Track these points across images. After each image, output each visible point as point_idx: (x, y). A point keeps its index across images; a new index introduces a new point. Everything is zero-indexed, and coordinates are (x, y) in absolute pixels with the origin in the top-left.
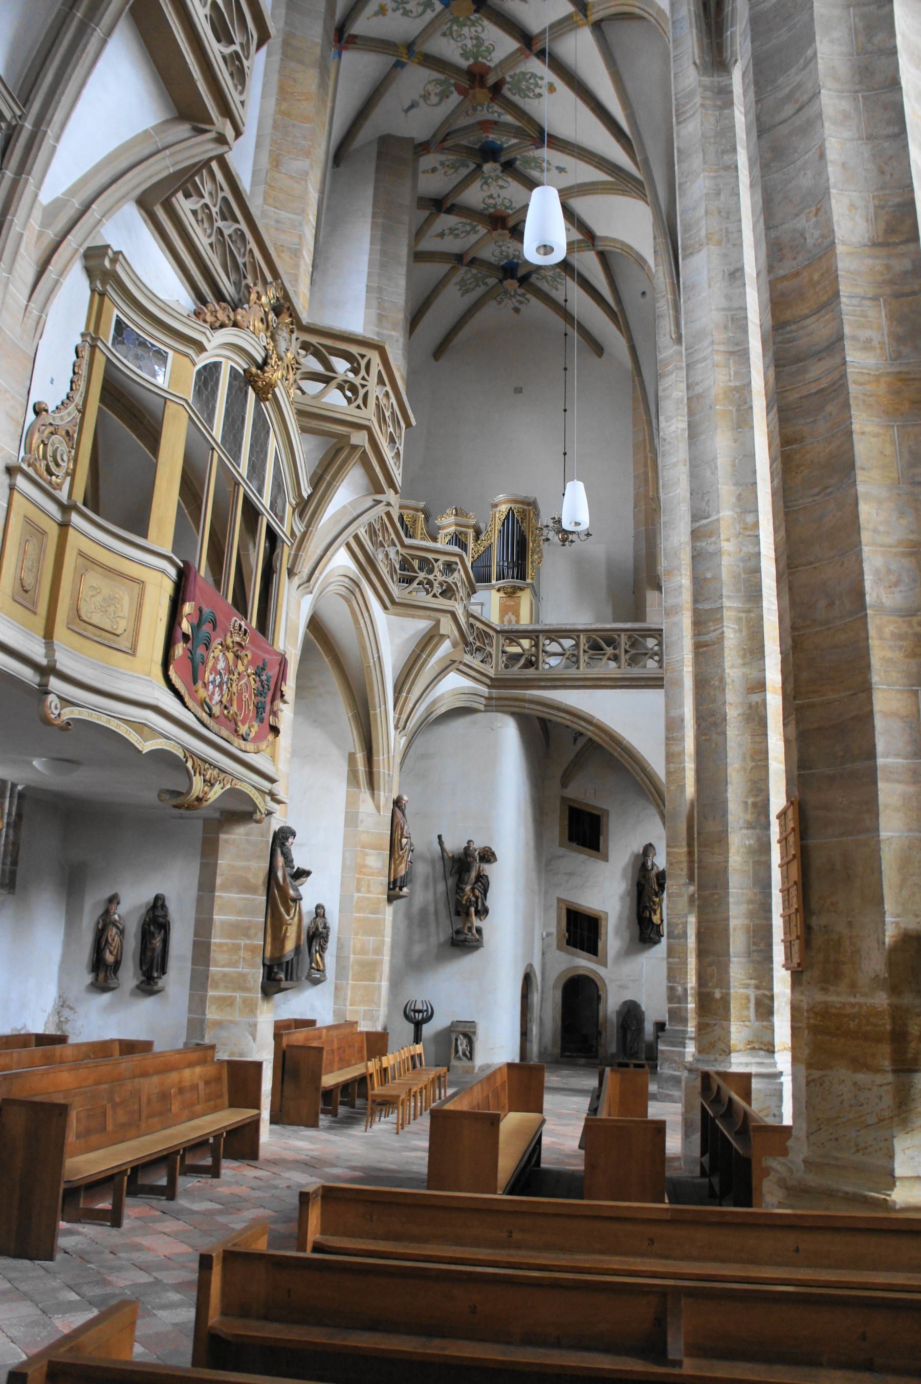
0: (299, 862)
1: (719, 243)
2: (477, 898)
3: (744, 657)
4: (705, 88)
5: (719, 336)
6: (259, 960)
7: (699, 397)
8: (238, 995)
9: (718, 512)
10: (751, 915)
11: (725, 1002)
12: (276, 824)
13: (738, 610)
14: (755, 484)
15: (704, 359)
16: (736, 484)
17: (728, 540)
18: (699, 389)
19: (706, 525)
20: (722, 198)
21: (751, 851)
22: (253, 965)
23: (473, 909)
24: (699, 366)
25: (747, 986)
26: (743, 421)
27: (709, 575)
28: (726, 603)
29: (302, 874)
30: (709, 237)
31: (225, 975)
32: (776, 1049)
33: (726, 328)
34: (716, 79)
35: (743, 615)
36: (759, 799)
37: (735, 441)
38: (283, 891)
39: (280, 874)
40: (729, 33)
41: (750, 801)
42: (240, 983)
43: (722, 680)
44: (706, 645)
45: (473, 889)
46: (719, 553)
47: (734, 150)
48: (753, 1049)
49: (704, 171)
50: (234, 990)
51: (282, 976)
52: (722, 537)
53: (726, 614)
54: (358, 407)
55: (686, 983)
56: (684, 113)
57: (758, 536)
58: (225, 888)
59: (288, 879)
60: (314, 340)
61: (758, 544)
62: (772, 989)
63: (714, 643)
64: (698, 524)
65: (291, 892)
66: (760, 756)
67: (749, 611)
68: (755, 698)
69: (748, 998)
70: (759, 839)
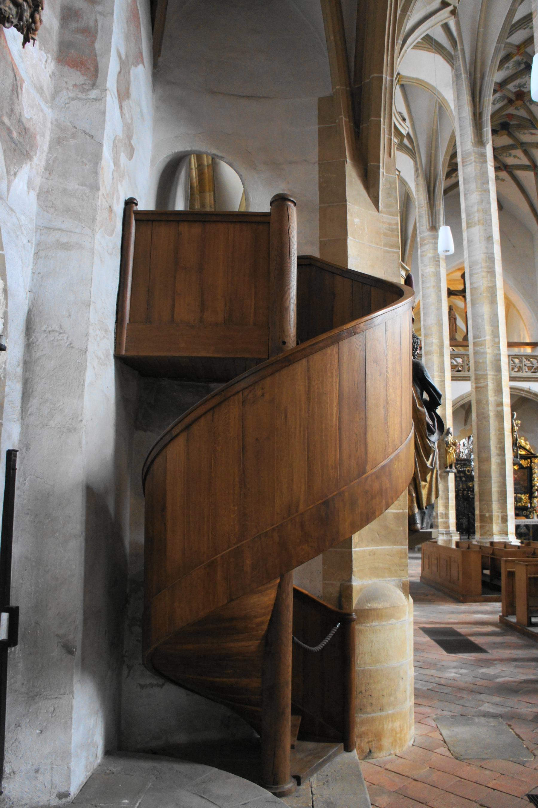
1: (483, 225)
3: (495, 393)
4: (475, 152)
5: (484, 265)
7: (475, 289)
9: (485, 337)
10: (499, 487)
11: (491, 518)
13: (493, 375)
14: (498, 326)
15: (477, 273)
16: (491, 326)
17: (489, 348)
18: (475, 285)
19: (479, 341)
20: (484, 204)
21: (499, 464)
24: (475, 275)
25: (498, 512)
26: (493, 301)
27: (481, 361)
28: (489, 372)
30: (479, 221)
32: (509, 533)
33: (486, 261)
34: (480, 149)
35: (495, 377)
36: (501, 445)
37: (491, 308)
40: (485, 129)
41: (498, 446)
43: (487, 401)
44: (480, 387)
46: (485, 353)
47: (488, 183)
48: (501, 534)
49: (476, 191)
53: (489, 377)
55: (438, 511)
56: (466, 162)
57: (499, 347)
62: (506, 513)
63: (484, 387)
64: (476, 340)
66: (501, 430)
67: (497, 376)
69: (499, 516)
70: (501, 460)
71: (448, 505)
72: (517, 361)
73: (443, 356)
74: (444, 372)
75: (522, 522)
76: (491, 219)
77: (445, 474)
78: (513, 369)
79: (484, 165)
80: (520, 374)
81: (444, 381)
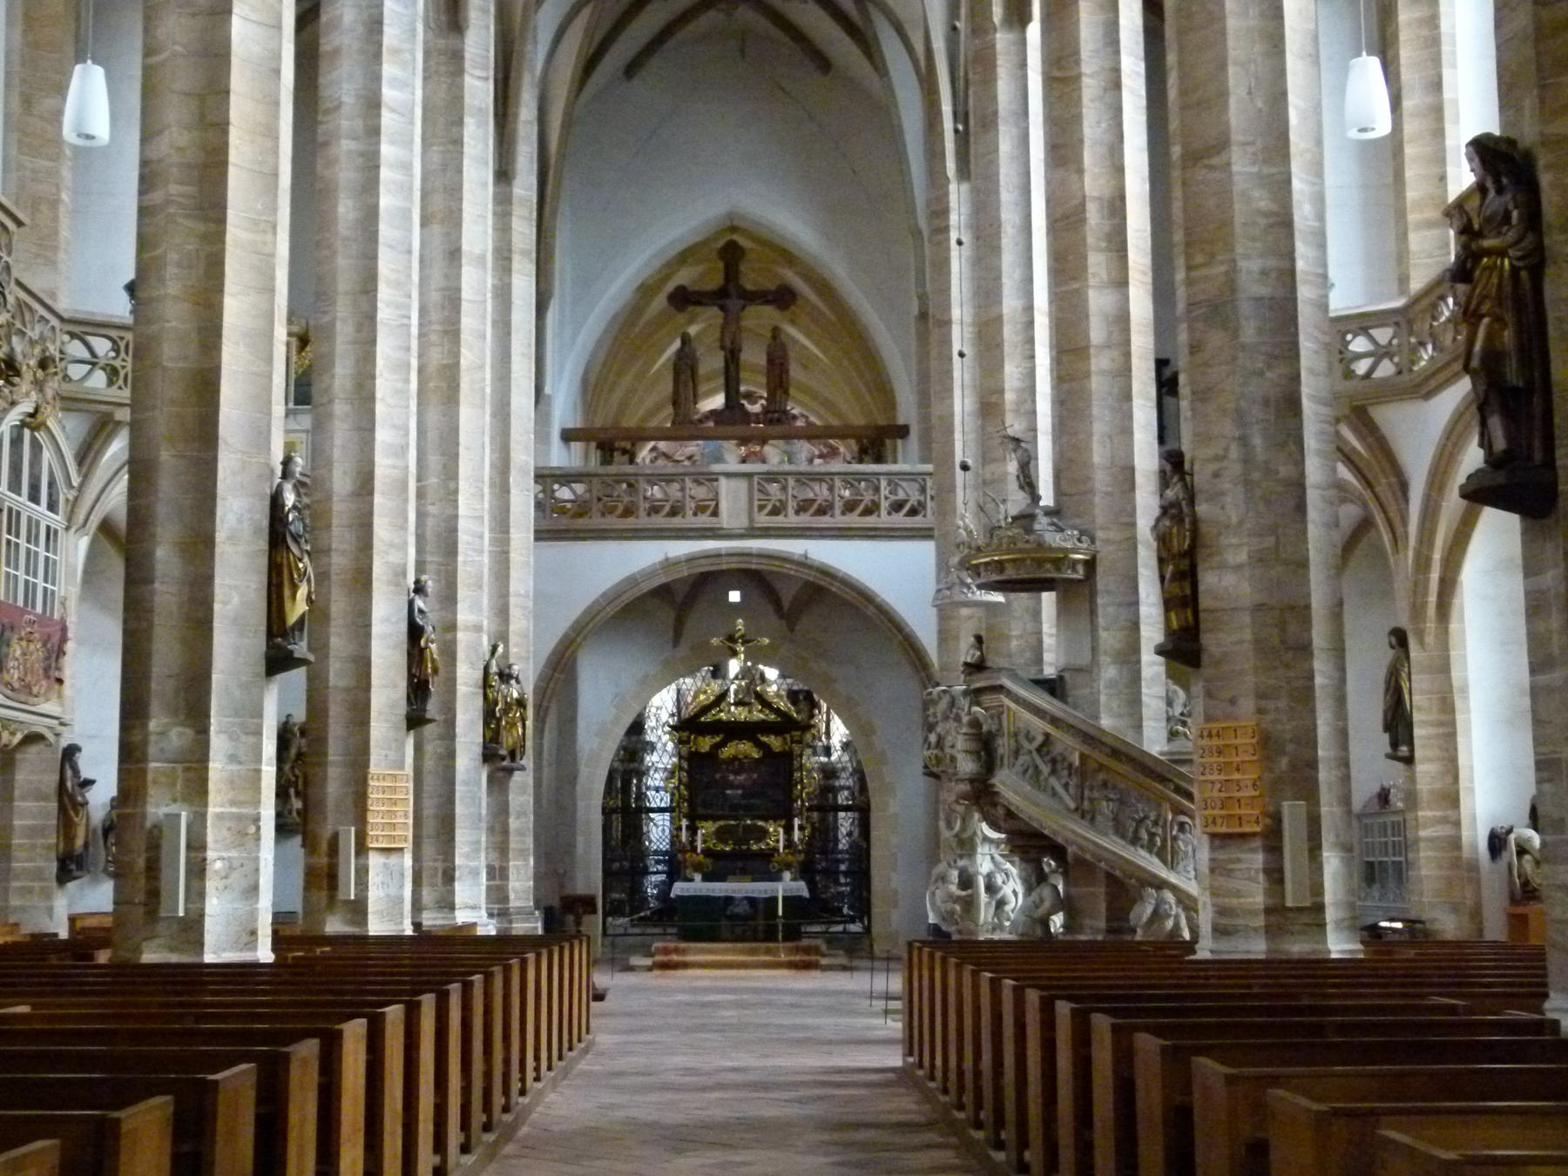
0: (85, 773)
1: (442, 222)
2: (297, 777)
3: (441, 602)
6: (53, 855)
8: (37, 885)
12: (64, 743)
14: (457, 455)
16: (443, 454)
17: (433, 504)
21: (441, 757)
22: (48, 860)
23: (292, 791)
29: (89, 783)
31: (24, 869)
33: (443, 308)
38: (72, 798)
39: (69, 784)
42: (38, 875)
45: (292, 768)
48: (440, 907)
50: (33, 880)
51: (73, 867)
52: (429, 501)
54: (120, 388)
57: (456, 501)
58: (24, 798)
59: (77, 788)
60: (77, 329)
61: (456, 507)
62: (453, 862)
65: (79, 799)
68: (448, 636)
71: (508, 848)
72: (774, 488)
73: (508, 492)
74: (507, 532)
75: (740, 891)
76: (460, 210)
77: (501, 774)
78: (761, 508)
79: (458, 79)
80: (778, 520)
81: (507, 552)
